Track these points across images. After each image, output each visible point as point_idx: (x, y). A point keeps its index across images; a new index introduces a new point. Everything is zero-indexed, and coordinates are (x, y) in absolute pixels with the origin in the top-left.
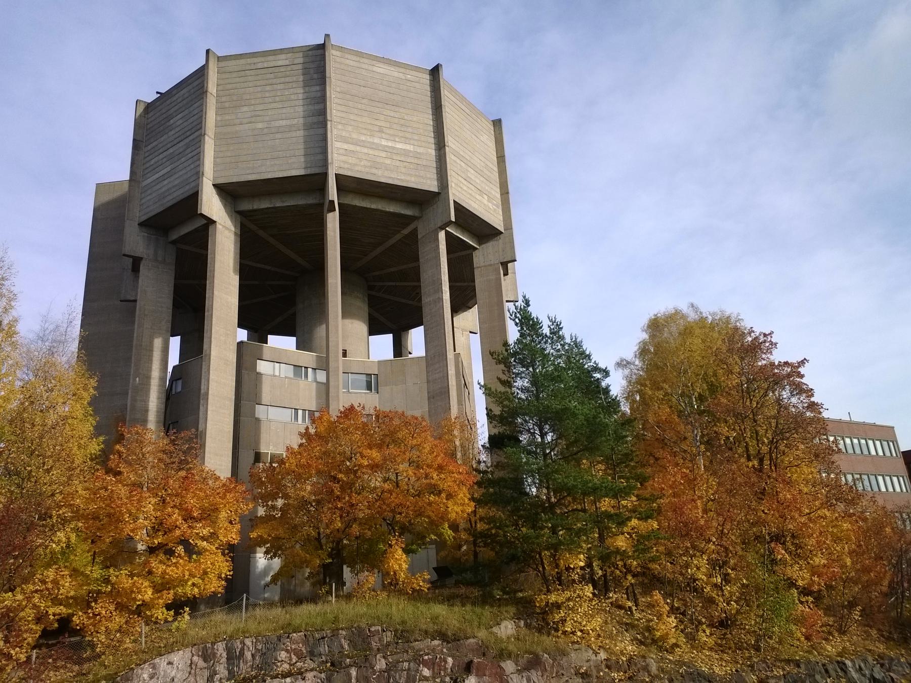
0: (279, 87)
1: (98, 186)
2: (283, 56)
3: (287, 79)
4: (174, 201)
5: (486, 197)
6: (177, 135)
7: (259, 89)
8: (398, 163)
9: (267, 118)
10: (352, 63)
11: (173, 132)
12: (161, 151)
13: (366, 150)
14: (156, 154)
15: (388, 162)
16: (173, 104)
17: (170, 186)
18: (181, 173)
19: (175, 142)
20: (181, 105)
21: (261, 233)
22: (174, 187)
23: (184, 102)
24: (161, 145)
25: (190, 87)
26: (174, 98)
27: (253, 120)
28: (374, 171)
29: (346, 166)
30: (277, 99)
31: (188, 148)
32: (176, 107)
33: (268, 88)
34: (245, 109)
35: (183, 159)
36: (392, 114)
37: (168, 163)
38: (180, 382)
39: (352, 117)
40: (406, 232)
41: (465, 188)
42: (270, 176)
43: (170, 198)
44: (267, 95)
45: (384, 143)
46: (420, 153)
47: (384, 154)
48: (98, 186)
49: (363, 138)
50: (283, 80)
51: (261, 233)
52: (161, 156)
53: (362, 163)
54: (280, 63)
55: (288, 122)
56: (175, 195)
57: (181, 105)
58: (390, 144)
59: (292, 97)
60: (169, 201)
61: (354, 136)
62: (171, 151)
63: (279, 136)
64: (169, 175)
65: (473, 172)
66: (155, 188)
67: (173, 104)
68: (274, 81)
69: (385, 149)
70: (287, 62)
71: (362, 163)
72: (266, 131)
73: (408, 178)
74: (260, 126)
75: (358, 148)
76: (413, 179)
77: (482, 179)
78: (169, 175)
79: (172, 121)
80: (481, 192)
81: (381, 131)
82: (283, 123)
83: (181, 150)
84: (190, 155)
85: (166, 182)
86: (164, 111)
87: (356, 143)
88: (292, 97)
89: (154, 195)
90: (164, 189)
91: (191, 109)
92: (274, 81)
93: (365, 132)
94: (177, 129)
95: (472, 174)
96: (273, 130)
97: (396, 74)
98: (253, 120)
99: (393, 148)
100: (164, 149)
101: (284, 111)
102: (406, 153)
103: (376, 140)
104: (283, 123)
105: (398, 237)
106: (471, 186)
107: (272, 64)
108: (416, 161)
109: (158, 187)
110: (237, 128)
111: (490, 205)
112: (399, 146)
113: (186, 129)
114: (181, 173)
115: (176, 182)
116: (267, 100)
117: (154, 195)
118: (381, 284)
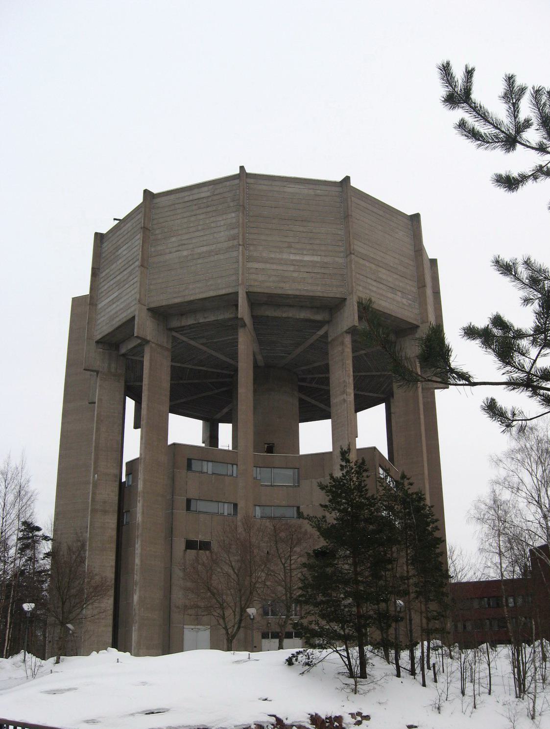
0: (202, 217)
1: (73, 299)
2: (206, 189)
3: (209, 209)
4: (120, 323)
5: (399, 294)
6: (123, 264)
7: (186, 220)
8: (305, 275)
9: (191, 246)
10: (264, 187)
11: (120, 261)
12: (111, 278)
13: (274, 267)
14: (108, 280)
15: (295, 275)
16: (121, 236)
17: (118, 308)
18: (125, 298)
19: (122, 270)
20: (126, 237)
21: (192, 343)
22: (119, 310)
23: (129, 234)
24: (112, 273)
25: (133, 221)
26: (122, 231)
27: (180, 248)
28: (282, 285)
29: (256, 284)
31: (131, 275)
32: (123, 239)
33: (193, 219)
34: (174, 239)
35: (127, 286)
36: (301, 229)
37: (117, 288)
38: (131, 476)
39: (263, 237)
40: (321, 332)
41: (374, 289)
42: (192, 298)
43: (117, 319)
44: (192, 225)
45: (292, 257)
46: (326, 263)
47: (292, 268)
48: (73, 299)
49: (273, 256)
50: (205, 210)
51: (192, 343)
52: (112, 282)
53: (271, 279)
54: (203, 195)
56: (121, 317)
57: (126, 237)
58: (298, 258)
59: (212, 225)
60: (116, 322)
61: (265, 255)
62: (118, 278)
63: (200, 261)
64: (117, 299)
65: (384, 271)
66: (108, 310)
67: (121, 236)
68: (198, 212)
69: (293, 263)
70: (208, 194)
71: (271, 279)
72: (190, 257)
74: (185, 253)
75: (268, 266)
77: (395, 276)
78: (117, 299)
79: (120, 251)
80: (393, 290)
81: (290, 247)
82: (204, 249)
83: (125, 278)
84: (132, 282)
85: (114, 306)
86: (114, 242)
87: (266, 261)
88: (212, 225)
89: (106, 317)
90: (113, 312)
91: (133, 241)
92: (198, 212)
94: (125, 258)
95: (383, 274)
96: (196, 257)
97: (306, 191)
98: (180, 248)
99: (301, 261)
100: (113, 276)
101: (205, 238)
102: (314, 264)
103: (285, 256)
104: (204, 249)
105: (315, 337)
106: (381, 286)
107: (196, 197)
108: (323, 271)
110: (167, 257)
111: (404, 301)
112: (307, 258)
113: (130, 259)
114: (125, 298)
115: (122, 306)
116: (191, 230)
118: (311, 376)
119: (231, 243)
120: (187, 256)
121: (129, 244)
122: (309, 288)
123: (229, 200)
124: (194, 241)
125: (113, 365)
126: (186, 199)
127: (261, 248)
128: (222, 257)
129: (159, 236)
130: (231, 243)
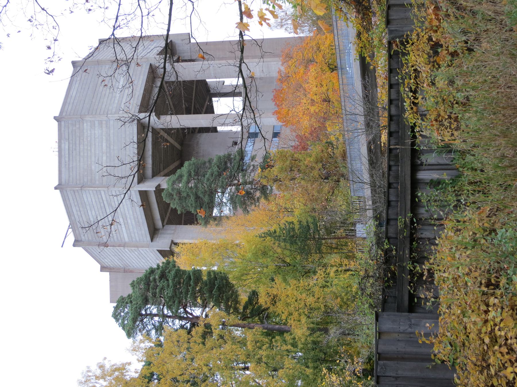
0: (82, 148)
2: (63, 145)
3: (78, 142)
7: (82, 159)
22: (133, 215)
30: (89, 148)
33: (82, 154)
34: (93, 167)
44: (86, 154)
49: (116, 101)
50: (78, 145)
54: (67, 147)
55: (104, 141)
59: (89, 139)
63: (112, 147)
70: (67, 143)
73: (141, 79)
76: (142, 77)
85: (129, 221)
88: (89, 139)
89: (135, 231)
91: (87, 203)
93: (112, 101)
97: (77, 85)
101: (97, 144)
104: (104, 145)
107: (67, 152)
109: (131, 227)
115: (131, 212)
117: (135, 231)
119: (104, 126)
120: (107, 157)
121: (88, 207)
122: (141, 82)
123: (74, 128)
124: (97, 152)
125: (169, 232)
126: (67, 159)
127: (111, 108)
128: (112, 131)
129: (89, 178)
130: (104, 126)
